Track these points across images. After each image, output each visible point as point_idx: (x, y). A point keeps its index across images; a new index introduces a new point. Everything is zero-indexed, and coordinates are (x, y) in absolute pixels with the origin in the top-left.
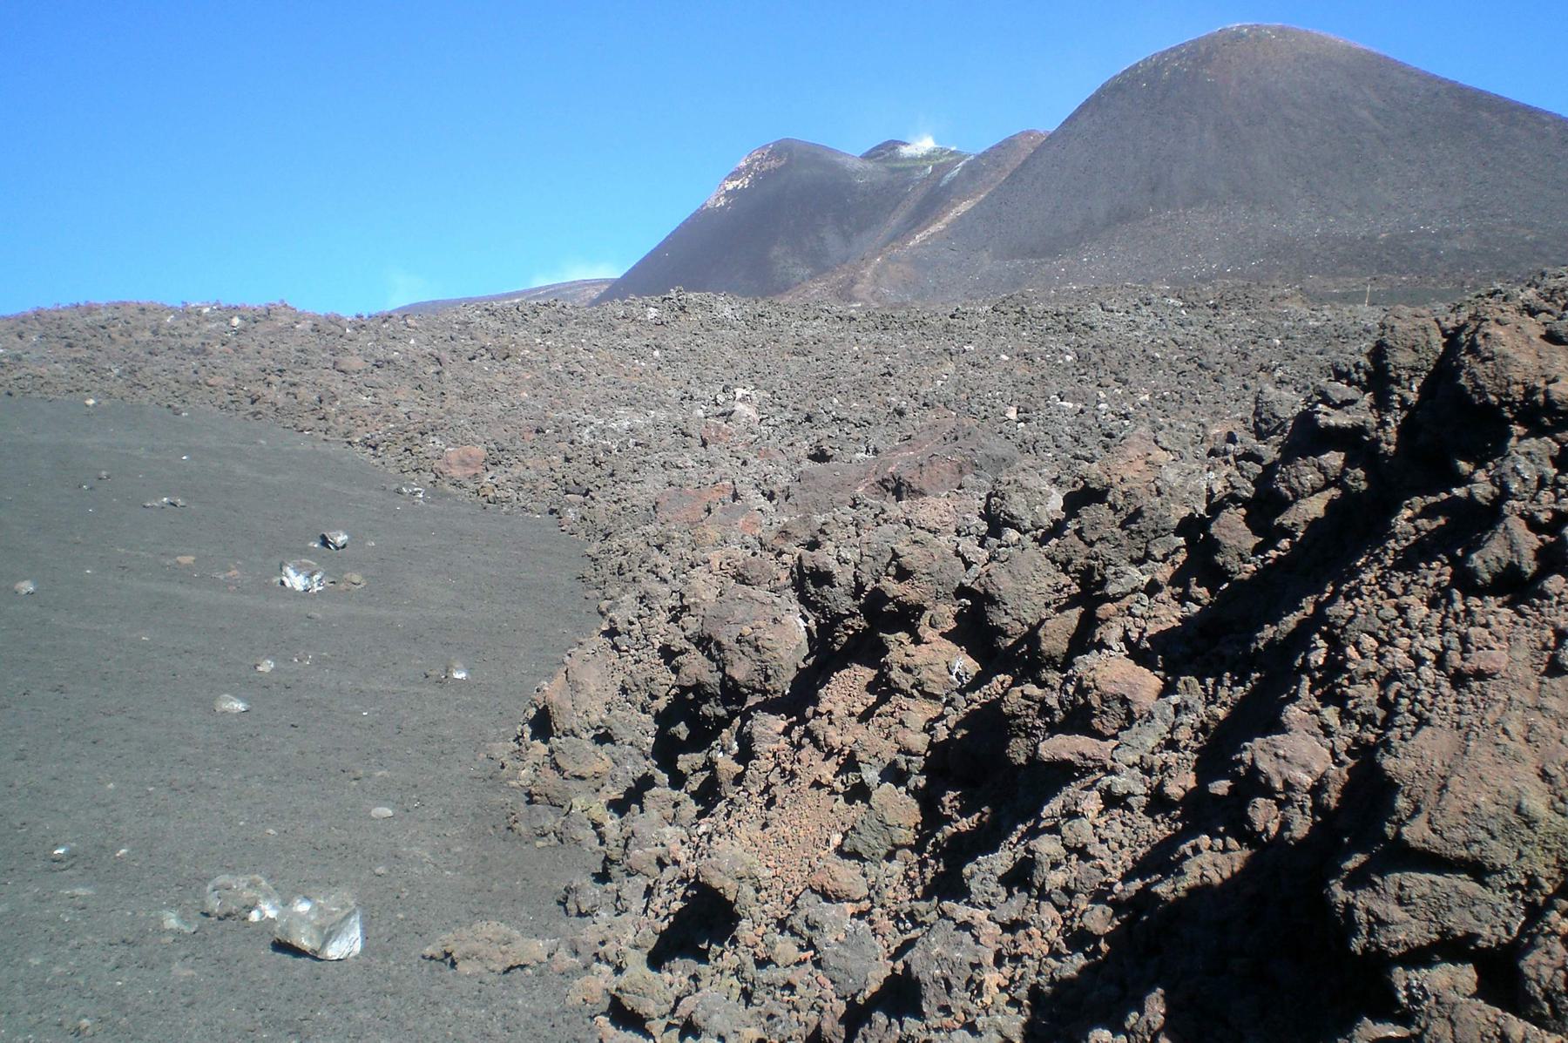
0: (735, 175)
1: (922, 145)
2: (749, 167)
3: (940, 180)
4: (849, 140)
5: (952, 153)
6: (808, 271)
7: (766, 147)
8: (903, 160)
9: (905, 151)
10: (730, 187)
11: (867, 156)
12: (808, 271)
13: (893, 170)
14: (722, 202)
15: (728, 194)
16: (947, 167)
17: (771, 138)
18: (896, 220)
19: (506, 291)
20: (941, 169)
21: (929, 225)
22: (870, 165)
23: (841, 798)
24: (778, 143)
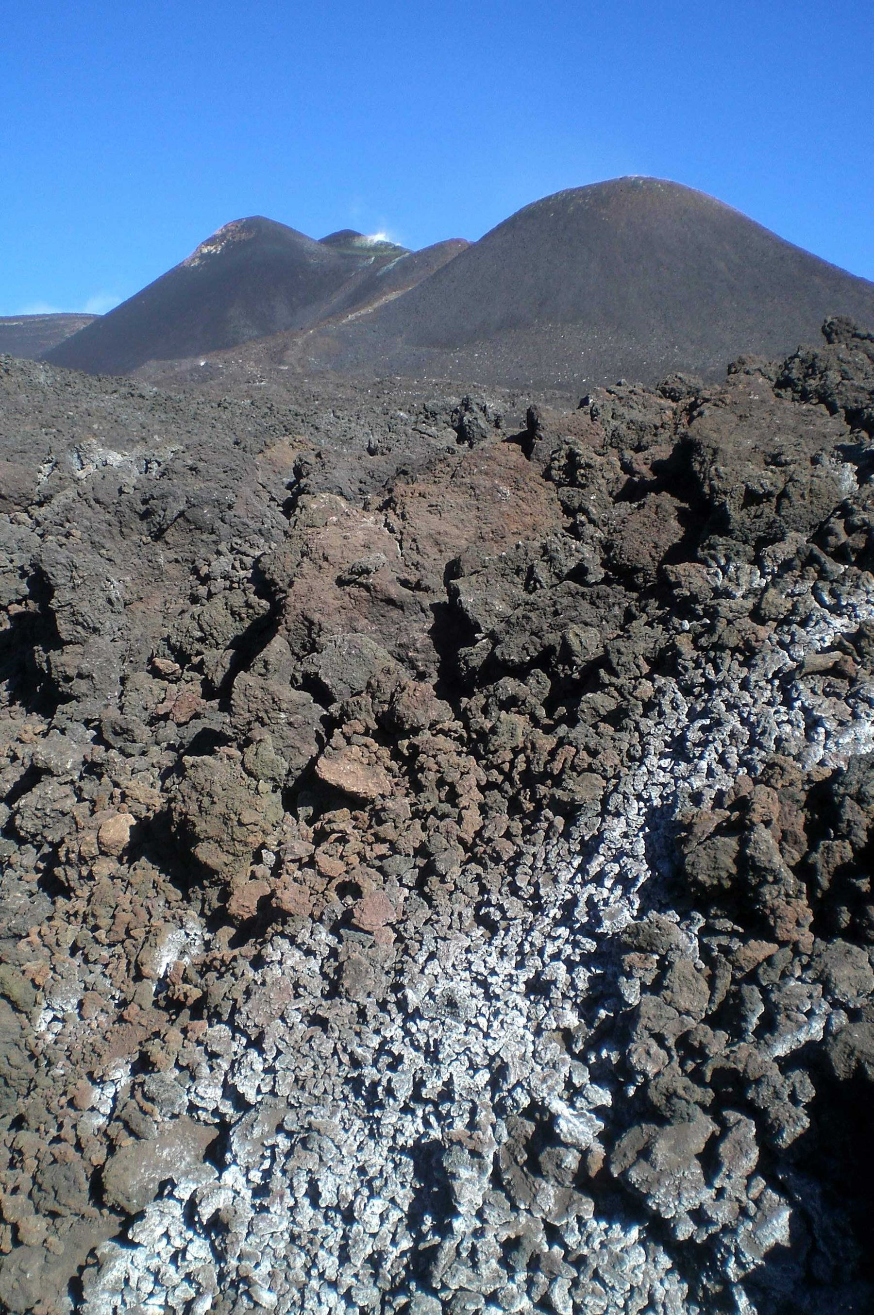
0: (211, 241)
1: (379, 237)
2: (223, 236)
3: (378, 270)
4: (313, 226)
5: (396, 248)
6: (255, 333)
7: (240, 221)
8: (354, 248)
9: (357, 243)
10: (205, 251)
11: (326, 241)
12: (255, 333)
13: (344, 256)
14: (197, 262)
15: (203, 257)
16: (388, 259)
17: (244, 214)
18: (336, 299)
19: (12, 314)
20: (382, 260)
21: (363, 307)
22: (324, 249)
23: (553, 609)
24: (247, 219)
